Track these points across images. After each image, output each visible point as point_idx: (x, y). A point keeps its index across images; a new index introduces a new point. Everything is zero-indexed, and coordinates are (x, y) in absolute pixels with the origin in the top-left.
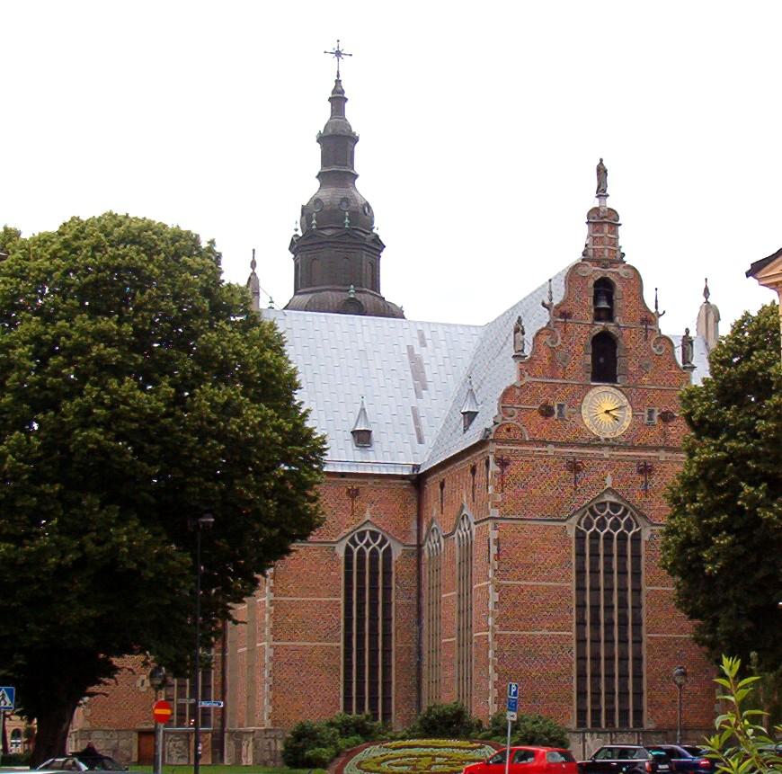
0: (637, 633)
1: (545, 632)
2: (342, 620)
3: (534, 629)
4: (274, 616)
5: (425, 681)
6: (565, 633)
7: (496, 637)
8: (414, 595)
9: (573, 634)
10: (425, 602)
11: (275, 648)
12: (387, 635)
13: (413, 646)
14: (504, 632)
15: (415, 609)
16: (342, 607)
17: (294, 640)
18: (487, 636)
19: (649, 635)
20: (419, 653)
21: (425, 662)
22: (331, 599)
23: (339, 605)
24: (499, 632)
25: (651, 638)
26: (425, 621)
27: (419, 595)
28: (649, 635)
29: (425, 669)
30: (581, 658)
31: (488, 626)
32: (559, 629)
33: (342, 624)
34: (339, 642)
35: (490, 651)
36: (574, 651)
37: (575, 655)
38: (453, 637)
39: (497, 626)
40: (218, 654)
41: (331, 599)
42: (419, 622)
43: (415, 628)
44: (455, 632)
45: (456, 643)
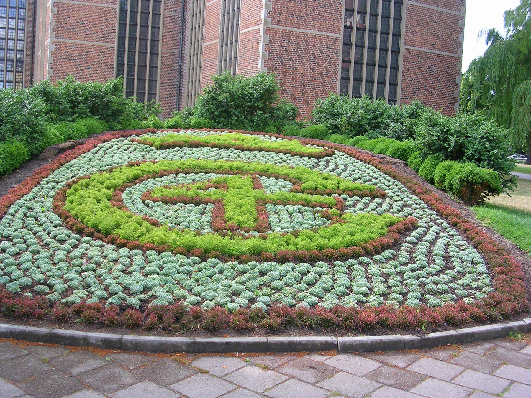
0: (396, 44)
1: (315, 31)
2: (117, 25)
3: (305, 27)
4: (56, 17)
5: (185, 81)
6: (334, 35)
7: (267, 30)
8: (179, 9)
9: (341, 36)
10: (189, 14)
11: (57, 44)
12: (155, 41)
13: (177, 51)
14: (276, 27)
15: (180, 21)
16: (118, 13)
17: (74, 39)
18: (259, 29)
19: (407, 47)
20: (182, 58)
21: (186, 65)
22: (108, 6)
23: (115, 12)
24: (270, 26)
25: (408, 50)
26: (188, 32)
27: (184, 9)
28: (407, 47)
29: (186, 71)
30: (346, 61)
31: (260, 20)
32: (328, 30)
33: (117, 28)
34: (113, 43)
35: (261, 45)
36: (340, 53)
37: (340, 58)
38: (217, 38)
39: (270, 20)
40: (27, 59)
41: (108, 6)
42: (183, 33)
43: (179, 37)
44: (219, 34)
45: (219, 44)
